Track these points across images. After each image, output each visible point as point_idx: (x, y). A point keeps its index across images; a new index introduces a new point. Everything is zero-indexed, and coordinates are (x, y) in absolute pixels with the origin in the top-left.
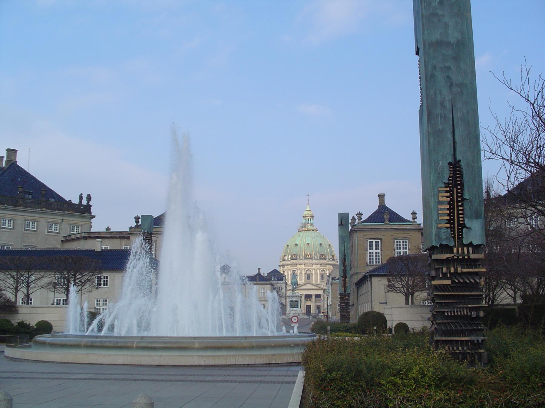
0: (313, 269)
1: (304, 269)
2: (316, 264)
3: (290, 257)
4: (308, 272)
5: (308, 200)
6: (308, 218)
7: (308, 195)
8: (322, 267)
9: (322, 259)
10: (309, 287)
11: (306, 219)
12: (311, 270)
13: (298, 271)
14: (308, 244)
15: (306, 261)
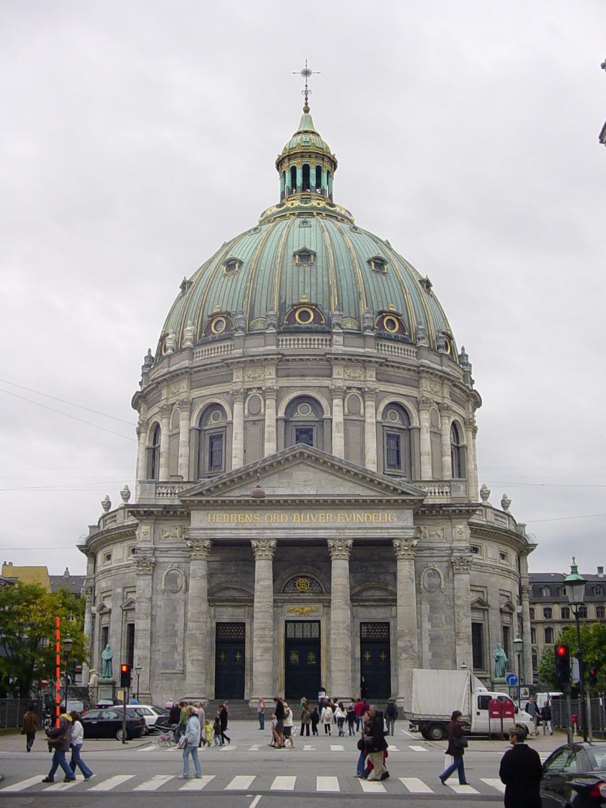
0: (331, 393)
1: (279, 394)
2: (351, 360)
3: (190, 331)
4: (304, 414)
5: (306, 95)
6: (306, 161)
7: (306, 73)
8: (390, 388)
9: (389, 338)
10: (306, 483)
11: (293, 170)
12: (324, 403)
13: (238, 407)
14: (305, 255)
15: (291, 345)
